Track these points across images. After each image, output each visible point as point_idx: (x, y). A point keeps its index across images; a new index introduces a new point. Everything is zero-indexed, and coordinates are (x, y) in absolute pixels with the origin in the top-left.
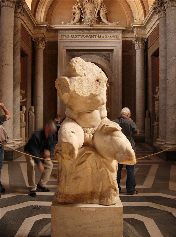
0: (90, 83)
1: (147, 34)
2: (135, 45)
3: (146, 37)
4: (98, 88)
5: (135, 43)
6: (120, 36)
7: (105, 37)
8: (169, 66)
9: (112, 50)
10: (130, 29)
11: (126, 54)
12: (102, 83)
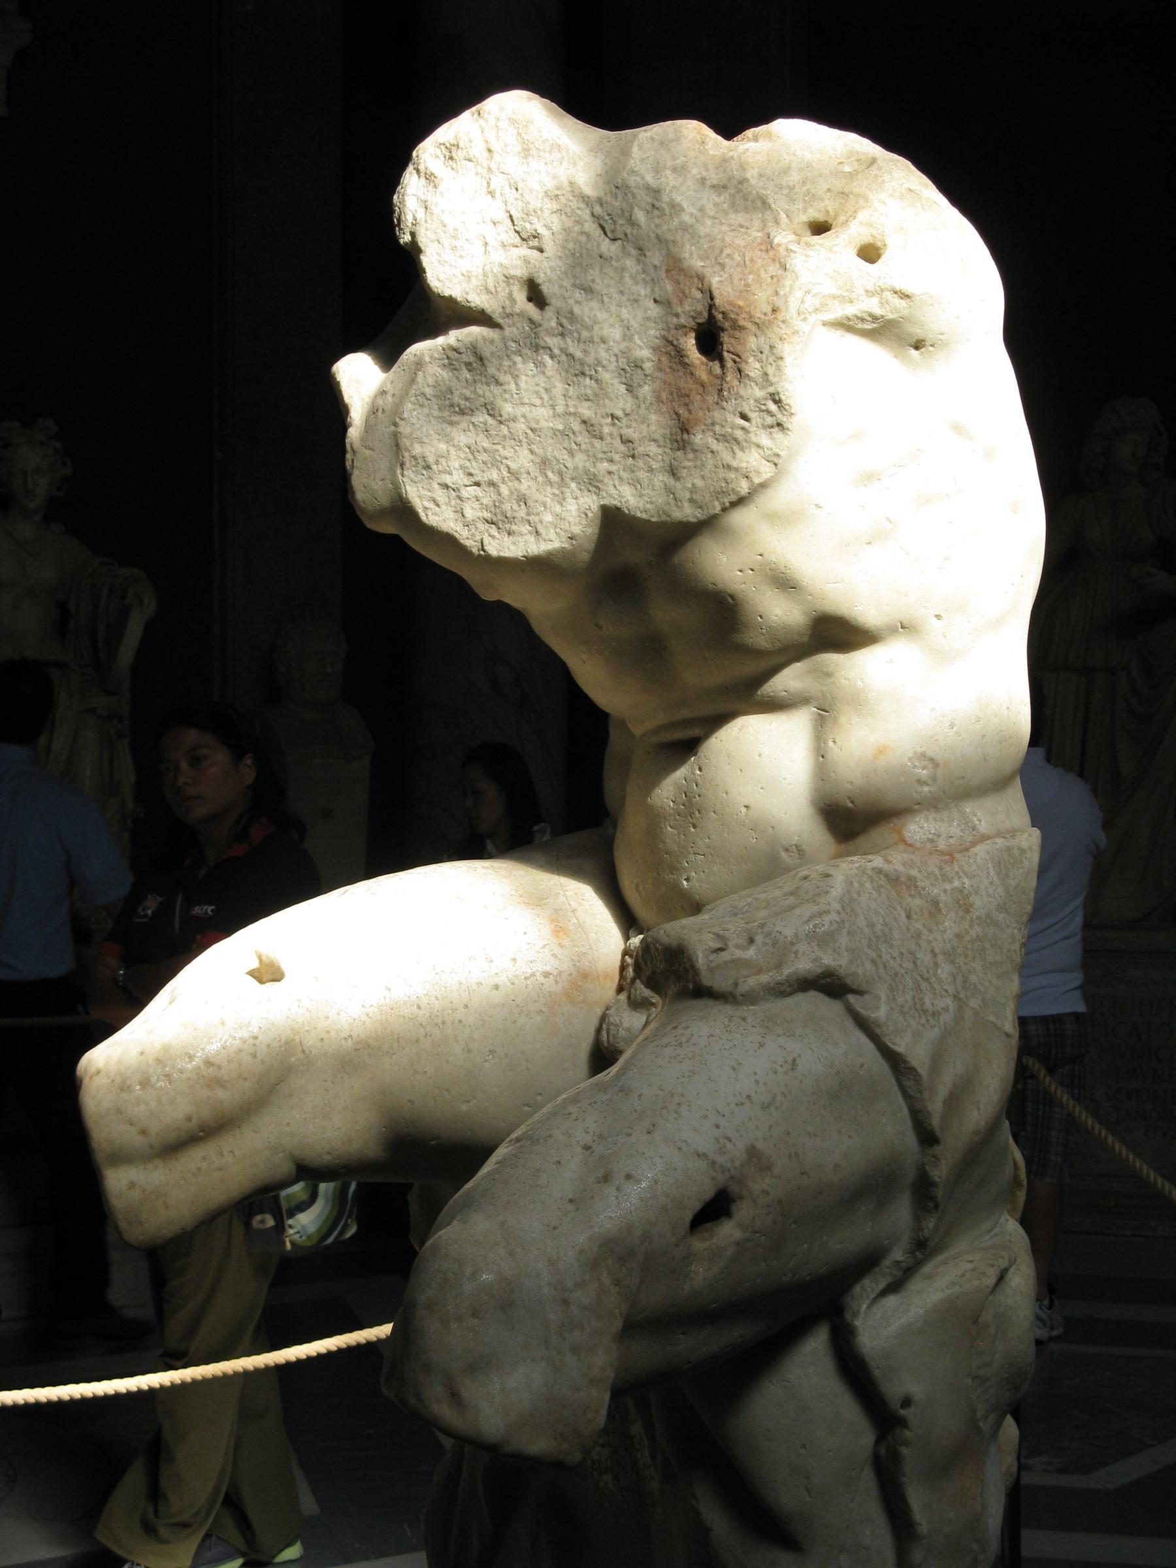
4: (698, 439)
12: (753, 368)
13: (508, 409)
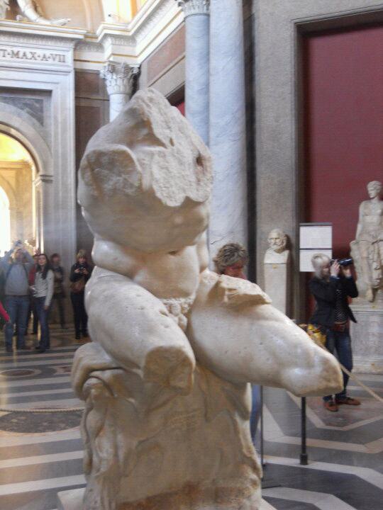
0: (183, 167)
1: (136, 57)
2: (108, 83)
3: (135, 63)
5: (109, 76)
6: (69, 56)
7: (29, 56)
8: (217, 137)
9: (49, 93)
10: (94, 40)
11: (83, 103)
13: (171, 170)
